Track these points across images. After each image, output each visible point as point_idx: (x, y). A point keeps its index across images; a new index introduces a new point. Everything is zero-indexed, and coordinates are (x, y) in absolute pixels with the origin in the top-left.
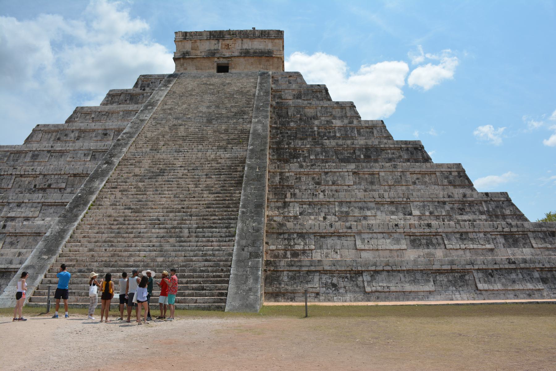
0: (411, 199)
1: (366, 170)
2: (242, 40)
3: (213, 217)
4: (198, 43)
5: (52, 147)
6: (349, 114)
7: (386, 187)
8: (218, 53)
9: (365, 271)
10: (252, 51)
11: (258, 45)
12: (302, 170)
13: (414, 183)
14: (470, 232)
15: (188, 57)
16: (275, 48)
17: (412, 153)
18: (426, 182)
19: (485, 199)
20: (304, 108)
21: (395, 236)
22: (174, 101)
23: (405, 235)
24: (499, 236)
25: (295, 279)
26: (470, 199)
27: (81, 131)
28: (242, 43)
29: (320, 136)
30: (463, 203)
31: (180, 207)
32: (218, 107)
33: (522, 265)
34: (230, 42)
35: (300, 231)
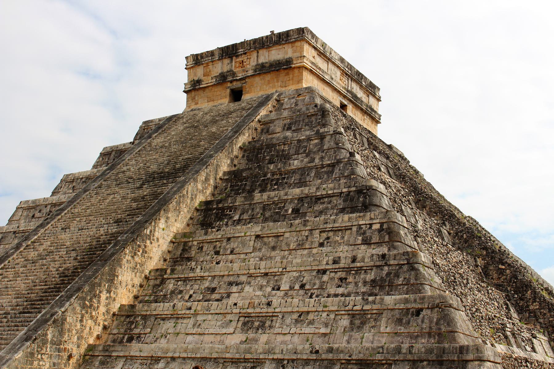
0: (288, 269)
2: (258, 52)
3: (38, 302)
4: (211, 67)
5: (18, 227)
7: (286, 253)
9: (164, 357)
11: (276, 54)
12: (205, 237)
13: (321, 245)
14: (312, 312)
15: (197, 87)
19: (378, 263)
21: (229, 317)
23: (240, 317)
24: (346, 317)
25: (104, 364)
26: (358, 265)
28: (257, 56)
30: (348, 270)
31: (26, 292)
33: (324, 356)
34: (244, 58)
35: (144, 313)
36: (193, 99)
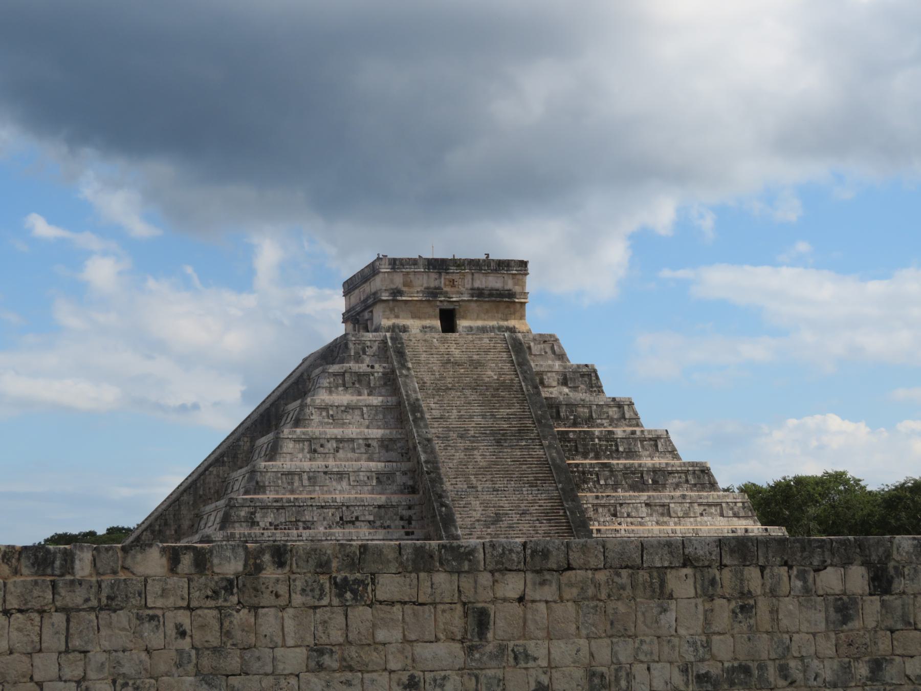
1: (657, 501)
2: (473, 274)
6: (627, 416)
8: (441, 293)
10: (486, 292)
11: (493, 282)
13: (702, 515)
16: (517, 289)
17: (699, 478)
18: (712, 513)
20: (576, 405)
22: (436, 400)
27: (339, 441)
28: (473, 279)
29: (602, 450)
32: (493, 416)
36: (392, 310)
